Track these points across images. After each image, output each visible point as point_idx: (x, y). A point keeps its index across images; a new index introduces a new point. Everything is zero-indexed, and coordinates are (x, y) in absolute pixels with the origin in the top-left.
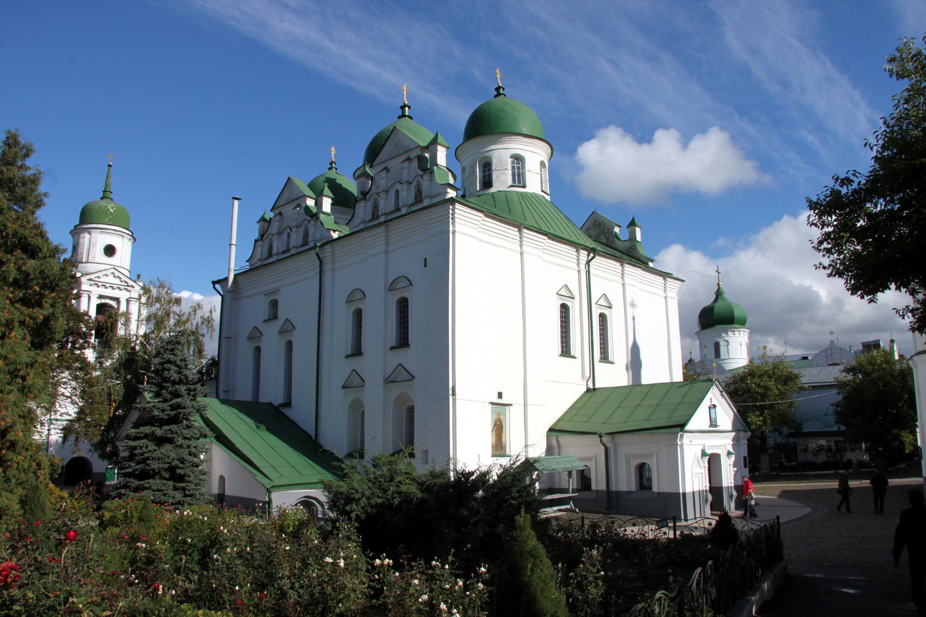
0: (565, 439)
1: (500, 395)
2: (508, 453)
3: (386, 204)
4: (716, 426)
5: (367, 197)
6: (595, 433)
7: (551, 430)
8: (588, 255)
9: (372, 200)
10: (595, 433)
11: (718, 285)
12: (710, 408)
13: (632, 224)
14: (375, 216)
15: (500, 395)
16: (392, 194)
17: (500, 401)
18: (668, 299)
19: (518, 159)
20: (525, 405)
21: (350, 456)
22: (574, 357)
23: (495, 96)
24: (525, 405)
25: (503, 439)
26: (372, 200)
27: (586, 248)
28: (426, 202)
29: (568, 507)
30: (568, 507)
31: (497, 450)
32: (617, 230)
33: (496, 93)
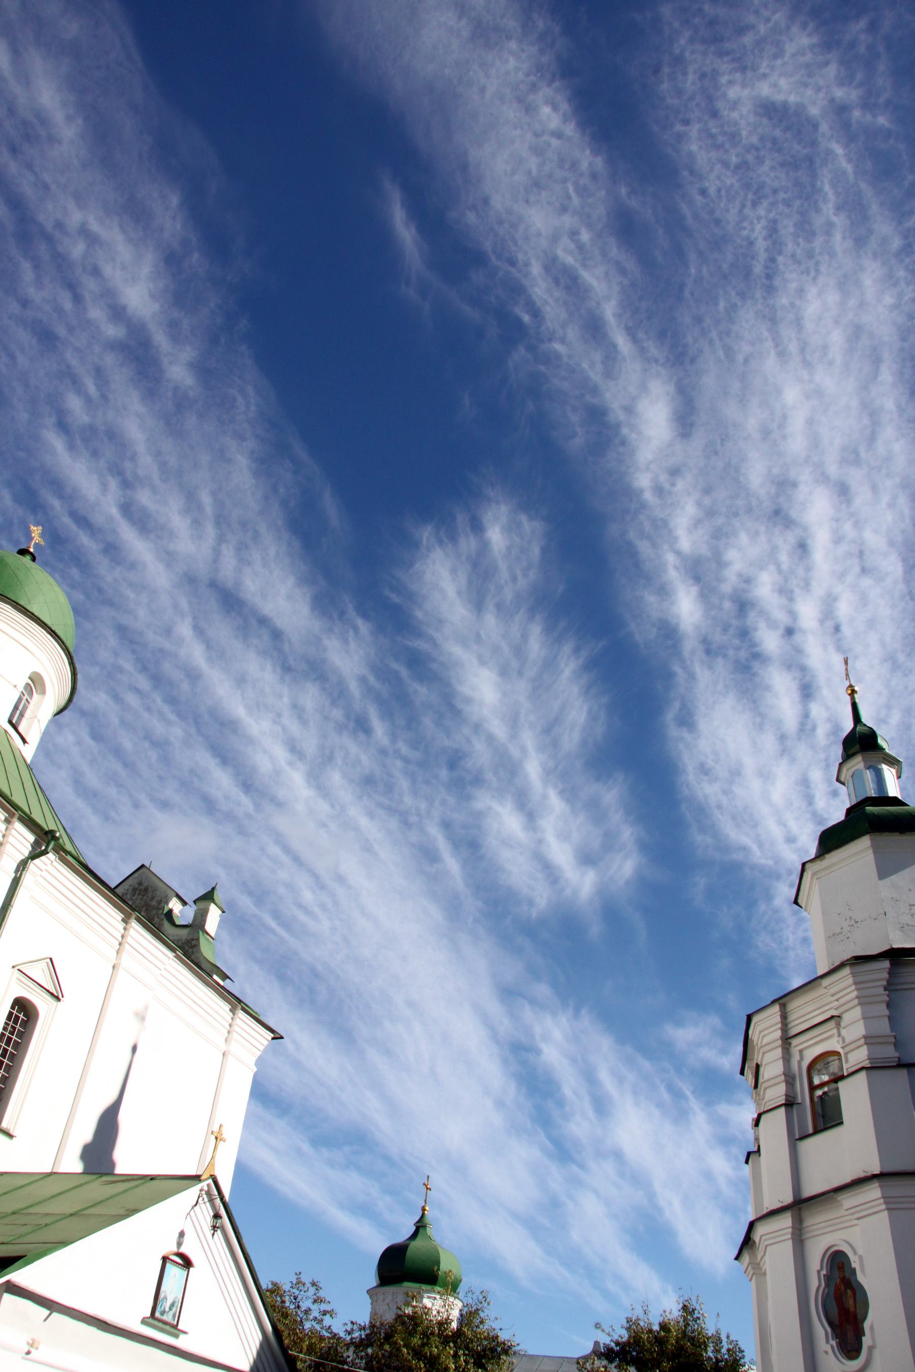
4: (174, 1329)
8: (36, 845)
11: (424, 1209)
12: (165, 1259)
13: (209, 897)
18: (230, 1059)
27: (30, 823)
32: (175, 905)
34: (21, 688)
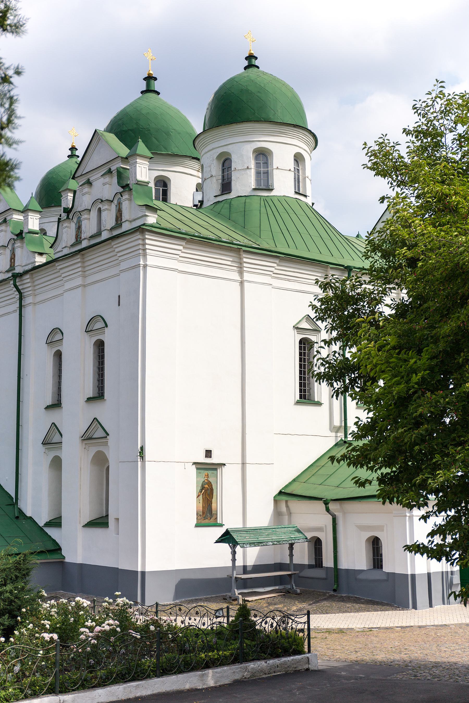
0: (295, 505)
1: (208, 453)
2: (219, 521)
3: (89, 227)
5: (71, 216)
6: (320, 499)
7: (281, 493)
9: (75, 220)
10: (320, 499)
14: (78, 240)
15: (208, 453)
16: (94, 214)
17: (208, 461)
19: (263, 155)
20: (244, 464)
21: (49, 524)
22: (319, 404)
23: (246, 68)
24: (244, 464)
25: (214, 505)
26: (75, 220)
28: (126, 227)
29: (289, 587)
30: (289, 587)
31: (205, 518)
33: (246, 63)
34: (293, 169)
